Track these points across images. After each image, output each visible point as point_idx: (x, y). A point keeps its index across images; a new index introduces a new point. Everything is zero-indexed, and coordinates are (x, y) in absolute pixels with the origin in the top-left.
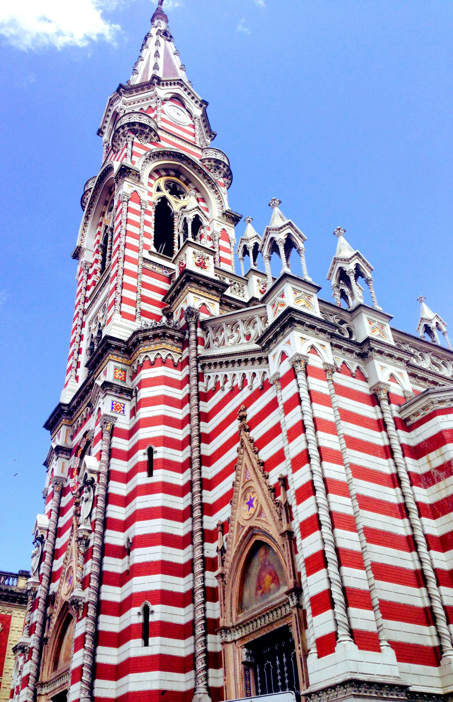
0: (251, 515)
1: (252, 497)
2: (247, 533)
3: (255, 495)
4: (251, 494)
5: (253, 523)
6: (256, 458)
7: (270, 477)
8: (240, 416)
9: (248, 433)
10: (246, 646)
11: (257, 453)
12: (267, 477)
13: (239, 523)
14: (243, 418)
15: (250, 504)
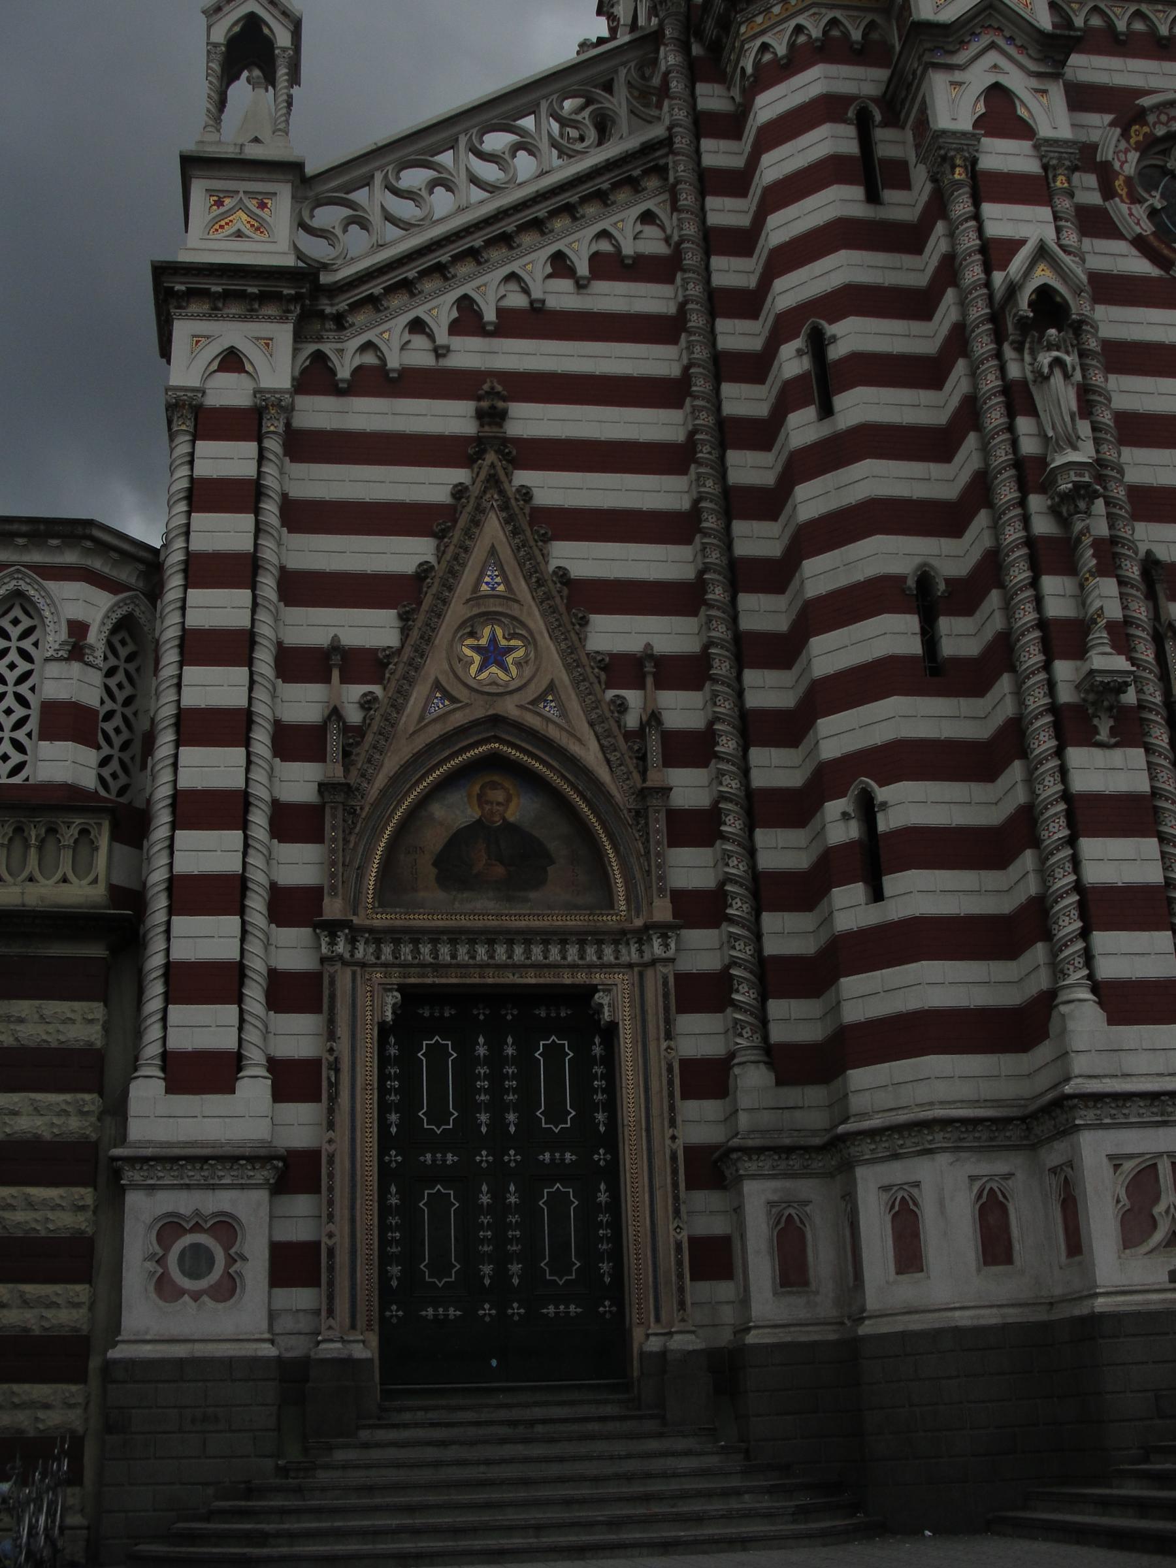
0: (494, 689)
1: (503, 643)
2: (475, 724)
3: (513, 643)
4: (499, 632)
5: (509, 708)
6: (545, 552)
7: (589, 629)
8: (493, 407)
9: (510, 468)
10: (401, 988)
11: (546, 539)
12: (584, 622)
13: (438, 685)
14: (492, 416)
15: (493, 655)
